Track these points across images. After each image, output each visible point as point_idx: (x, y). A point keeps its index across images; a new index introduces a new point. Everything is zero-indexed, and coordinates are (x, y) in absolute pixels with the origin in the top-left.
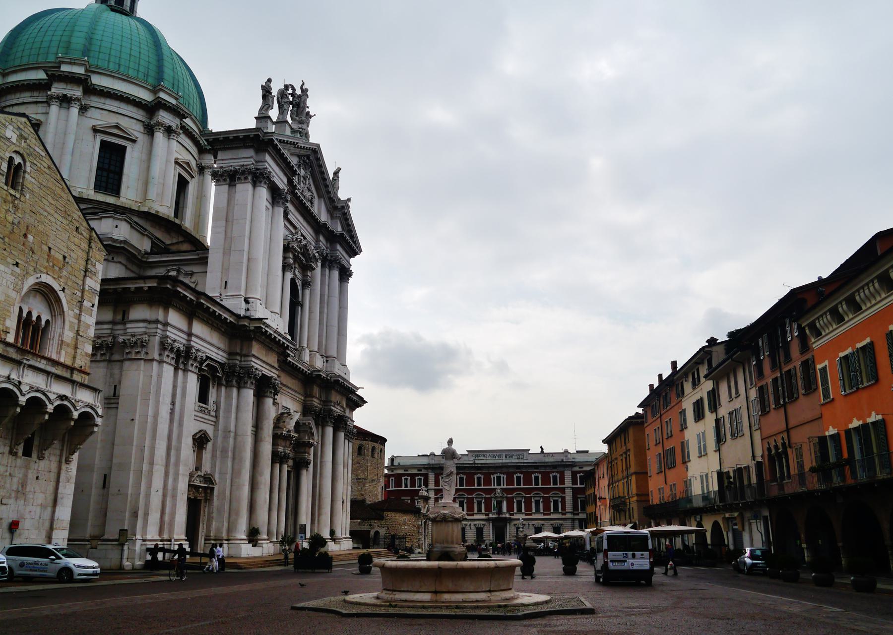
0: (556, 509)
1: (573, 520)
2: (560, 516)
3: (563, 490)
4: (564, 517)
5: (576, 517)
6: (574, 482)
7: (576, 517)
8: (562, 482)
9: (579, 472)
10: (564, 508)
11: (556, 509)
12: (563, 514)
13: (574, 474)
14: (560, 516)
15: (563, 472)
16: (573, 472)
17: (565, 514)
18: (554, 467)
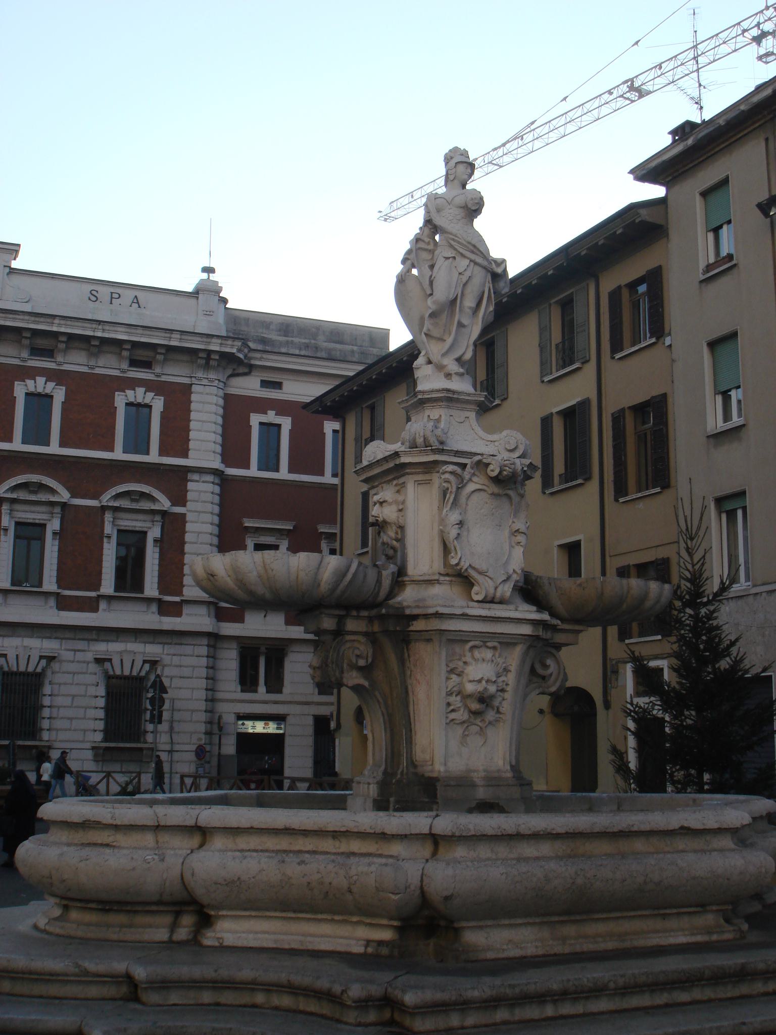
0: (130, 575)
1: (214, 639)
2: (149, 619)
3: (175, 481)
4: (169, 623)
5: (230, 629)
6: (234, 447)
7: (230, 629)
8: (176, 436)
9: (262, 405)
10: (171, 577)
11: (130, 575)
12: (165, 609)
13: (235, 411)
14: (149, 619)
15: (186, 390)
16: (229, 399)
17: (174, 610)
18: (142, 354)
